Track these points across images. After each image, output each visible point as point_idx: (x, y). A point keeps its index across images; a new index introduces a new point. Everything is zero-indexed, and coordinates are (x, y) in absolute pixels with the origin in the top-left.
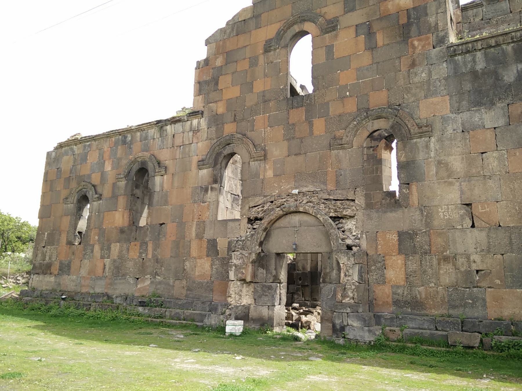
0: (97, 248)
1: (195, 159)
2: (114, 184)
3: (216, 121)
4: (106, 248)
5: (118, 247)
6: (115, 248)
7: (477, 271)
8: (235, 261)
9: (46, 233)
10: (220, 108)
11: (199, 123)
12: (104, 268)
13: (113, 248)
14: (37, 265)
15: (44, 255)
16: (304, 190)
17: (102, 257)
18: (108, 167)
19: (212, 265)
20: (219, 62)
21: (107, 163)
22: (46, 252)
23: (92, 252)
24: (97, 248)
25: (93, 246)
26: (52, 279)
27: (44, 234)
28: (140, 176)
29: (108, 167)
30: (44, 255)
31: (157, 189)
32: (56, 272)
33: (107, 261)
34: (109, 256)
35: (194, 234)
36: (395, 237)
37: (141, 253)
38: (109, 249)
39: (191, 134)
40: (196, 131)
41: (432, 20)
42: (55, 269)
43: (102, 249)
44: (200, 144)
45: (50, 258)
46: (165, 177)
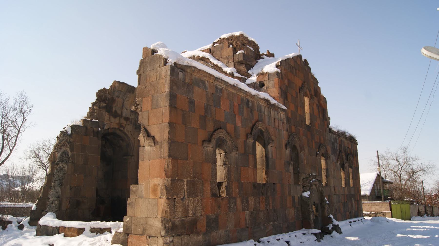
0: (239, 201)
1: (284, 142)
2: (245, 142)
4: (245, 201)
5: (253, 201)
6: (251, 201)
9: (185, 181)
13: (250, 202)
14: (177, 222)
15: (186, 210)
17: (244, 210)
19: (295, 212)
21: (237, 117)
22: (188, 206)
23: (235, 205)
24: (239, 201)
25: (235, 198)
26: (200, 237)
27: (183, 181)
30: (186, 210)
32: (204, 230)
33: (247, 212)
34: (248, 208)
35: (287, 193)
37: (266, 205)
38: (247, 202)
42: (202, 225)
43: (242, 202)
45: (194, 214)
46: (273, 148)
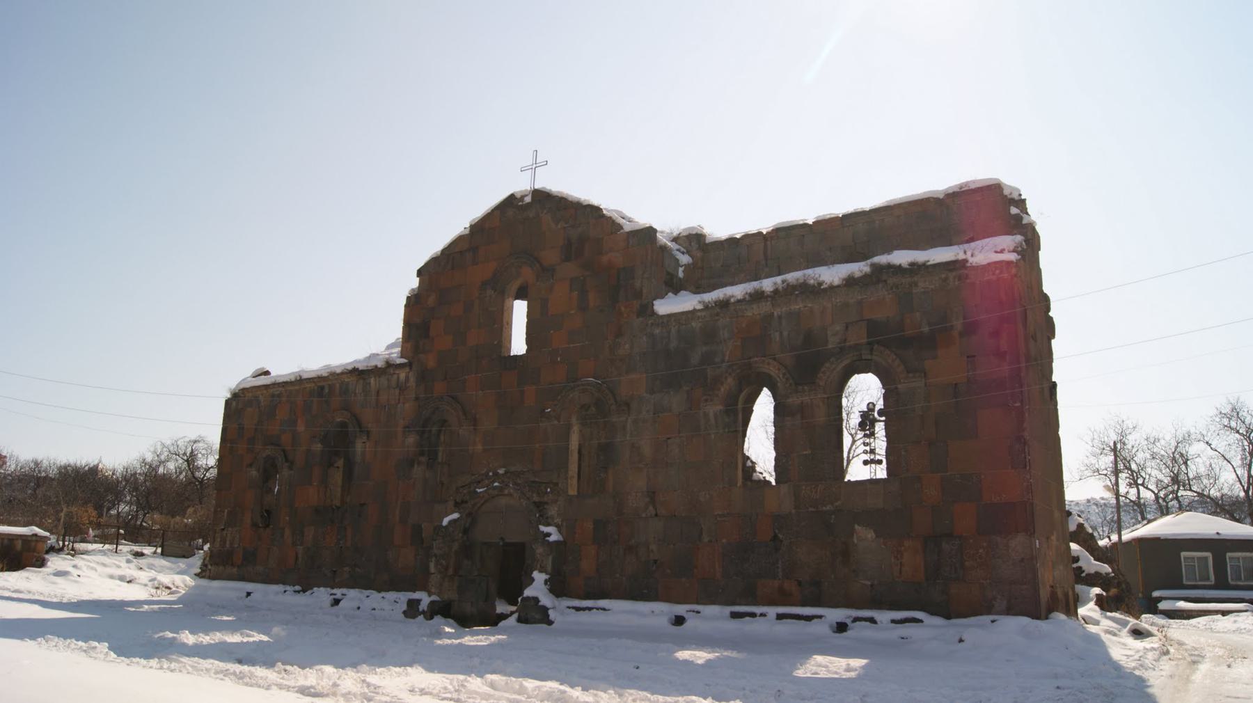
0: (287, 532)
3: (424, 377)
7: (655, 561)
8: (435, 551)
10: (431, 362)
11: (407, 378)
12: (297, 558)
16: (512, 469)
18: (301, 428)
20: (431, 301)
24: (287, 532)
28: (338, 443)
29: (301, 428)
31: (358, 459)
36: (589, 526)
39: (397, 391)
40: (402, 388)
41: (638, 284)
44: (407, 405)
